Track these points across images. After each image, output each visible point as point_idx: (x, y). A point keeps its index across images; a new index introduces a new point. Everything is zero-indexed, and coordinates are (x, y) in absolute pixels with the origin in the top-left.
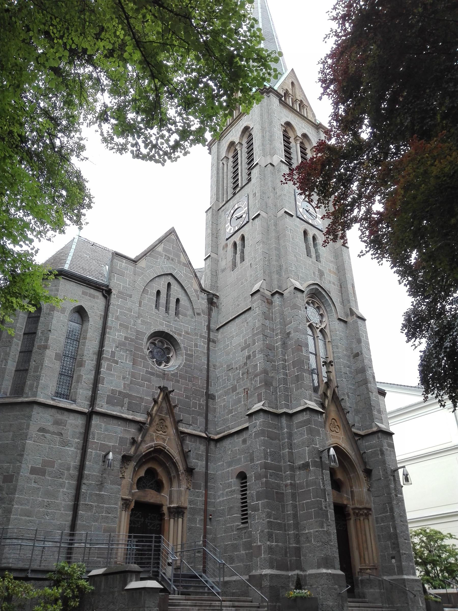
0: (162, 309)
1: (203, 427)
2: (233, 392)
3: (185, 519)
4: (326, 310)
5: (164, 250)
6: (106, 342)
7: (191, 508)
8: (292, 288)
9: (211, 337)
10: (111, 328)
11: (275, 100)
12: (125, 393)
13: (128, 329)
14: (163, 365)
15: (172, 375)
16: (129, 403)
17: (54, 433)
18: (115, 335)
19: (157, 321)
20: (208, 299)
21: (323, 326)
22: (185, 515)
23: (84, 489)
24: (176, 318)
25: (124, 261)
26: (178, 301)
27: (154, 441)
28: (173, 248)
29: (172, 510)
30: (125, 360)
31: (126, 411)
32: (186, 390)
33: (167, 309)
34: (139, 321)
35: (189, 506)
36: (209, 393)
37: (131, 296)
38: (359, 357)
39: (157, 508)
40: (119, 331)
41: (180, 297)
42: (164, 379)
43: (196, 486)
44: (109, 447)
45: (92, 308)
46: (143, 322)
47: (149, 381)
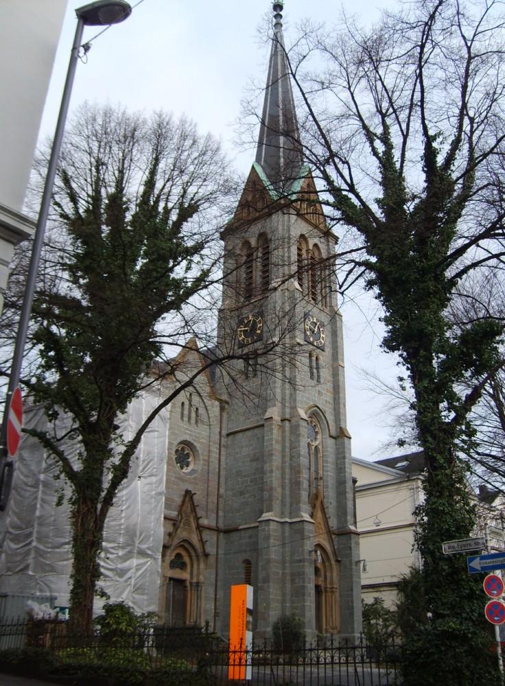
0: (186, 419)
21: (317, 443)
33: (189, 418)
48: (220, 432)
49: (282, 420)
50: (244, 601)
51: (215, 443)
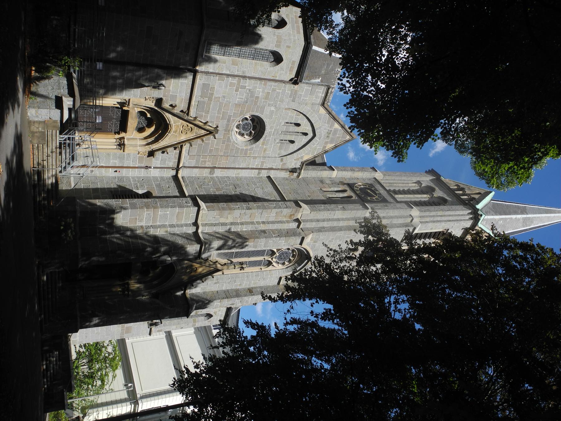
1: (187, 165)
2: (216, 189)
3: (116, 151)
4: (287, 268)
5: (336, 130)
6: (253, 81)
7: (124, 155)
8: (304, 236)
9: (263, 171)
10: (265, 84)
11: (468, 224)
12: (212, 98)
13: (265, 99)
15: (229, 137)
16: (204, 102)
18: (260, 89)
19: (274, 124)
20: (295, 168)
21: (274, 264)
22: (119, 150)
24: (278, 141)
25: (323, 95)
26: (292, 142)
27: (174, 123)
28: (339, 137)
29: (122, 140)
31: (198, 100)
32: (217, 149)
34: (273, 108)
35: (125, 153)
36: (215, 170)
37: (293, 101)
38: (248, 293)
39: (123, 127)
40: (263, 92)
41: (296, 143)
42: (225, 130)
43: (141, 159)
44: (169, 87)
45: (282, 69)
46: (272, 112)
47: (222, 119)
48: (272, 169)
49: (297, 220)
50: (100, 129)
51: (263, 163)
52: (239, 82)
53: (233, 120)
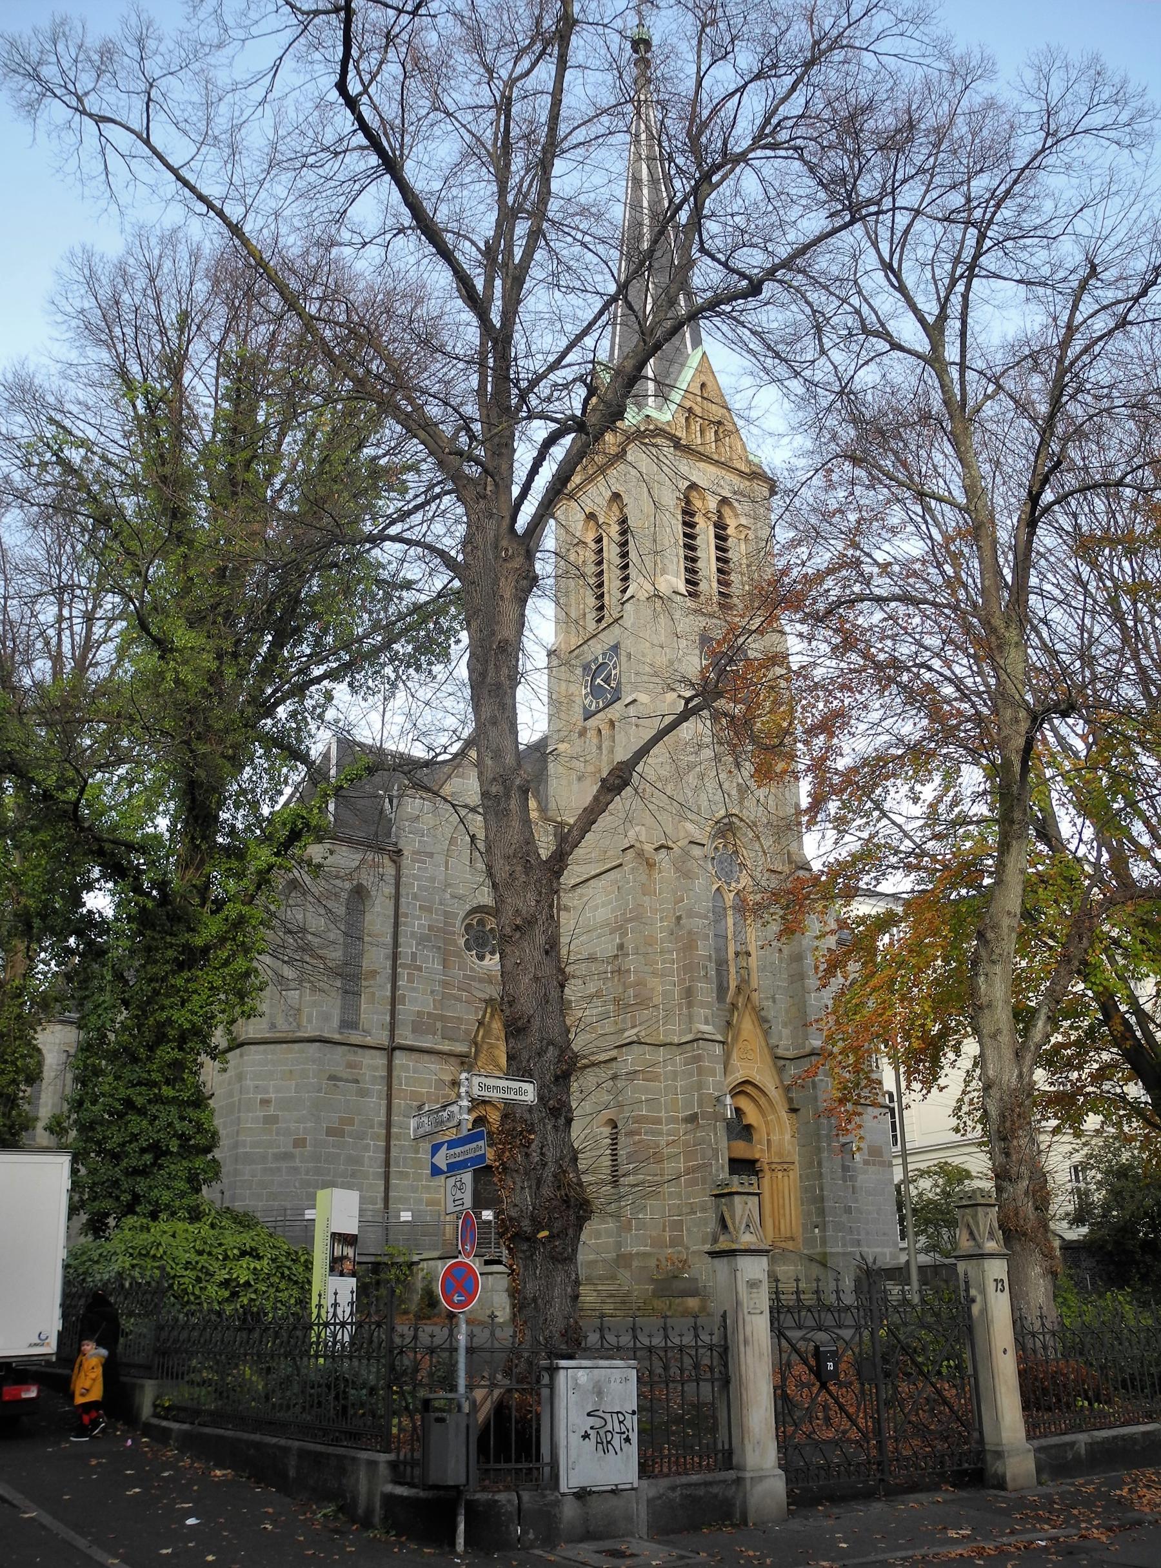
6: (401, 940)
10: (406, 915)
14: (488, 957)
17: (347, 1081)
18: (416, 923)
21: (740, 886)
23: (394, 1153)
30: (432, 963)
52: (404, 966)
53: (472, 969)
